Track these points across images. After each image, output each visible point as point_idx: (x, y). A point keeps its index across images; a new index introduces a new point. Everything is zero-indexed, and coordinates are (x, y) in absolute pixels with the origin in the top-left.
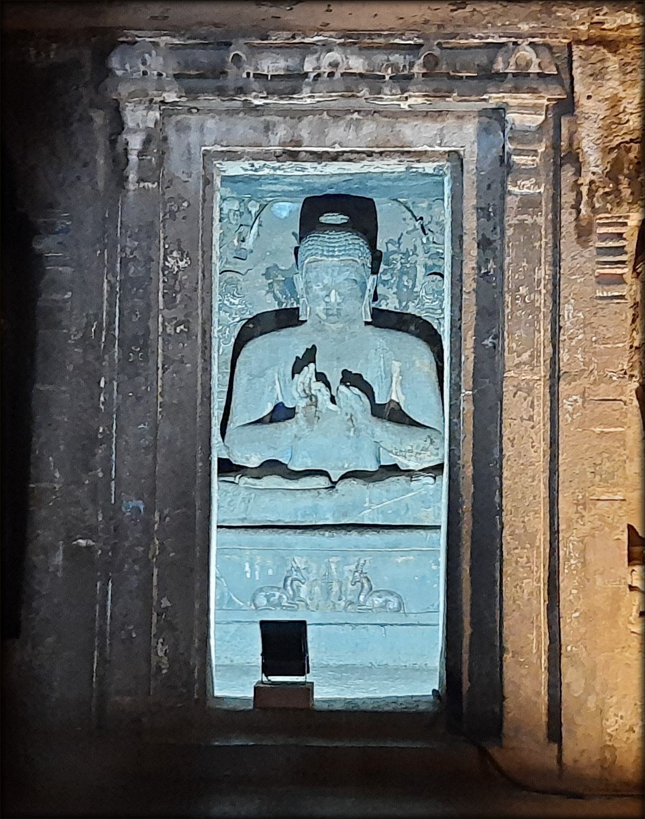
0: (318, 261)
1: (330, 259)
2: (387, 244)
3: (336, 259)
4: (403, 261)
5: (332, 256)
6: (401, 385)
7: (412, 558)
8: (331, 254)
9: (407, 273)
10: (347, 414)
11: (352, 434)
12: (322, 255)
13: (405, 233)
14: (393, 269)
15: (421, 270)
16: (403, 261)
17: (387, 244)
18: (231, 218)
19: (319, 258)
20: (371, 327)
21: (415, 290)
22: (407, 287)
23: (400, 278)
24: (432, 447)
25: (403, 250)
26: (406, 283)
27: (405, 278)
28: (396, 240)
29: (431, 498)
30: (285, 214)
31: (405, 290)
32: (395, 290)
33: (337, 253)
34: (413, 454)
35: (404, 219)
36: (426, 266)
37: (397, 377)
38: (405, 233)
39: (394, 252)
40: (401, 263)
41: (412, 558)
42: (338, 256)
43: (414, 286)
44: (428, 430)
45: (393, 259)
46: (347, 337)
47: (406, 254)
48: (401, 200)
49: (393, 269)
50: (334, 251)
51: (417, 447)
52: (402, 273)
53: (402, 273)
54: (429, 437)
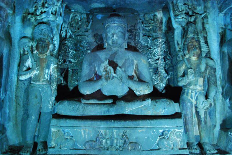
0: (110, 25)
1: (114, 24)
3: (116, 24)
5: (115, 23)
7: (144, 130)
8: (114, 23)
10: (119, 77)
11: (121, 84)
12: (111, 23)
14: (133, 34)
15: (141, 35)
17: (131, 27)
18: (84, 19)
19: (110, 24)
20: (126, 50)
21: (140, 40)
22: (137, 40)
24: (148, 89)
26: (137, 39)
27: (137, 37)
28: (134, 25)
29: (150, 107)
30: (100, 18)
32: (133, 41)
33: (116, 22)
34: (142, 91)
36: (143, 33)
37: (136, 66)
39: (133, 29)
40: (135, 33)
41: (144, 130)
42: (116, 23)
43: (139, 39)
44: (146, 83)
46: (119, 52)
48: (135, 14)
50: (115, 22)
51: (144, 89)
54: (147, 85)
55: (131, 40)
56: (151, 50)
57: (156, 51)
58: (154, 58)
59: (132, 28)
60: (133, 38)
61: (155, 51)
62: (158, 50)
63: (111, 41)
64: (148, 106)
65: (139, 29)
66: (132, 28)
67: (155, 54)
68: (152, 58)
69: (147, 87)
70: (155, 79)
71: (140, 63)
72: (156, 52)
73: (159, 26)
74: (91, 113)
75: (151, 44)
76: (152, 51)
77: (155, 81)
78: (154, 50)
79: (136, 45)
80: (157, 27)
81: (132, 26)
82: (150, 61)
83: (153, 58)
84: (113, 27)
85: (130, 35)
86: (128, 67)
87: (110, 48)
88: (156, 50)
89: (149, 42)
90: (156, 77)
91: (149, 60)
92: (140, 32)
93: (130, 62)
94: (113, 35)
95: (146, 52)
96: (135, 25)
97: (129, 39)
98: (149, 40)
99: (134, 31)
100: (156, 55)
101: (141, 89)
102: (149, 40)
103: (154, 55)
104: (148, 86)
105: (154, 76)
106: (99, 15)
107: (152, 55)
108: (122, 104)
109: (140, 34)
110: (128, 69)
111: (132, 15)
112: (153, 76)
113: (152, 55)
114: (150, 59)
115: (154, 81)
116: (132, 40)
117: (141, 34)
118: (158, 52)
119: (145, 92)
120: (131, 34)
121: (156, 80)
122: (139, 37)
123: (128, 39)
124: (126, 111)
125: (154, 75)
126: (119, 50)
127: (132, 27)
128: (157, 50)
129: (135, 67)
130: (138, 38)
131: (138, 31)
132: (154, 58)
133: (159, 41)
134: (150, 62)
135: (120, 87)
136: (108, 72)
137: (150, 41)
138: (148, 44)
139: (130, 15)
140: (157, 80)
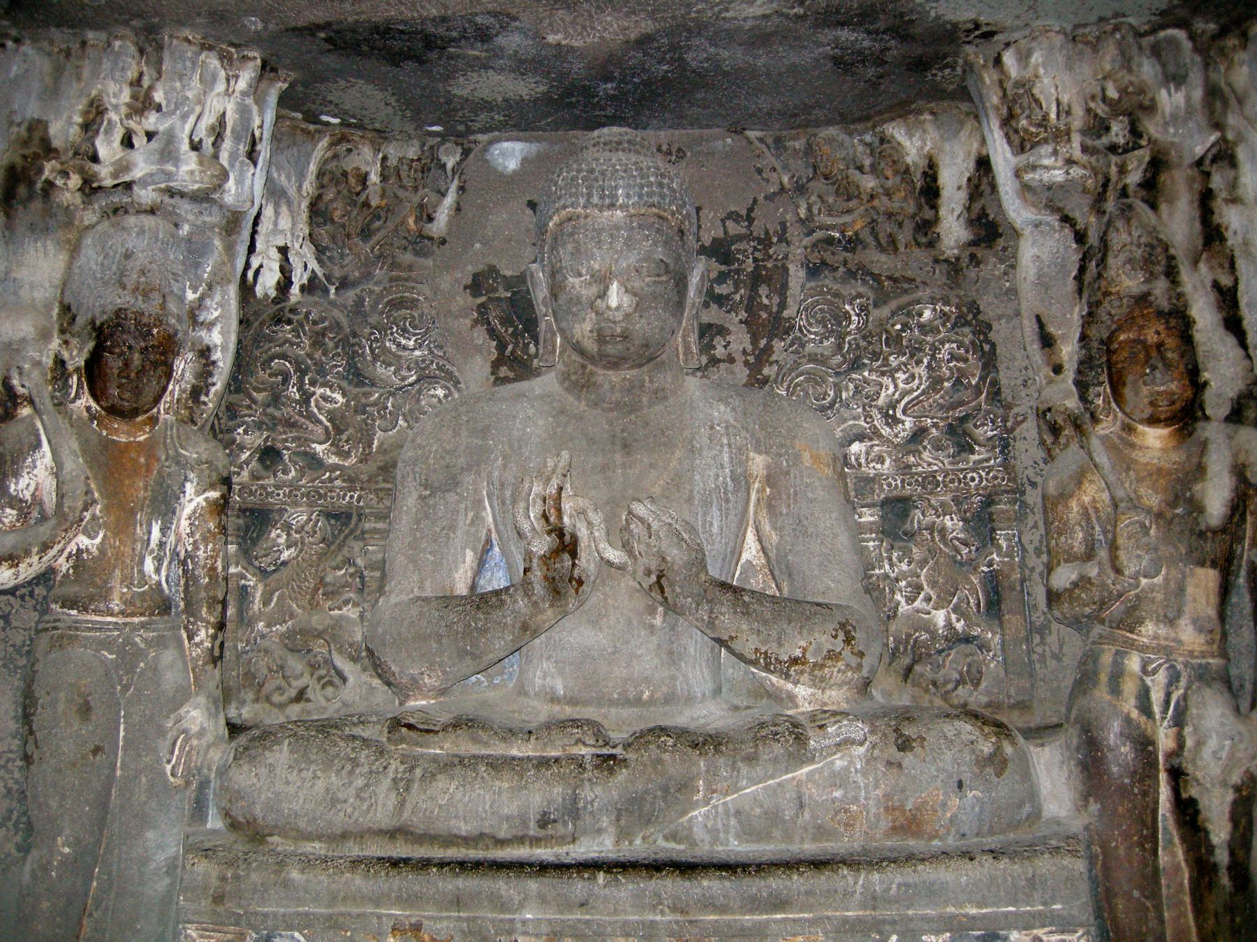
0: (578, 217)
2: (723, 220)
4: (757, 254)
5: (612, 206)
6: (770, 507)
9: (768, 280)
10: (648, 573)
11: (658, 621)
13: (761, 197)
16: (757, 254)
18: (403, 174)
21: (786, 314)
23: (754, 288)
25: (758, 229)
26: (765, 301)
27: (763, 290)
28: (744, 212)
30: (512, 165)
31: (764, 315)
32: (743, 315)
35: (760, 171)
38: (761, 197)
39: (740, 238)
40: (755, 260)
43: (783, 305)
45: (738, 251)
47: (765, 242)
49: (738, 271)
52: (757, 279)
53: (757, 279)
55: (728, 312)
56: (866, 381)
57: (901, 385)
58: (886, 431)
59: (734, 228)
60: (738, 297)
61: (892, 389)
62: (913, 377)
63: (587, 326)
64: (847, 769)
65: (782, 239)
66: (734, 228)
67: (893, 405)
68: (876, 433)
69: (841, 636)
70: (897, 580)
71: (788, 473)
72: (902, 396)
73: (913, 216)
74: (453, 823)
75: (864, 338)
76: (869, 390)
77: (898, 597)
78: (886, 380)
79: (763, 343)
80: (900, 225)
81: (734, 216)
82: (857, 460)
83: (880, 436)
84: (599, 232)
85: (722, 278)
86: (707, 504)
87: (584, 367)
88: (901, 376)
89: (853, 327)
90: (904, 567)
91: (856, 447)
92: (786, 257)
93: (722, 466)
94: (602, 281)
95: (832, 393)
96: (751, 210)
97: (714, 307)
98: (847, 307)
99: (746, 251)
100: (899, 415)
101: (798, 653)
102: (847, 307)
103: (886, 415)
104: (847, 633)
105: (890, 559)
106: (506, 145)
107: (875, 413)
108: (666, 756)
109: (786, 270)
110: (705, 514)
111: (729, 140)
112: (880, 559)
113: (875, 413)
114: (861, 437)
115: (893, 592)
116: (733, 309)
117: (792, 268)
118: (912, 391)
119: (826, 670)
120: (723, 268)
121: (903, 584)
122: (783, 290)
123: (706, 305)
124: (695, 805)
125: (887, 551)
126: (642, 386)
127: (730, 224)
128: (907, 382)
129: (758, 500)
130: (776, 300)
131: (771, 251)
132: (886, 431)
133: (920, 315)
134: (863, 461)
135: (655, 639)
136: (567, 538)
137: (854, 318)
138: (841, 337)
139: (719, 143)
140: (909, 585)
